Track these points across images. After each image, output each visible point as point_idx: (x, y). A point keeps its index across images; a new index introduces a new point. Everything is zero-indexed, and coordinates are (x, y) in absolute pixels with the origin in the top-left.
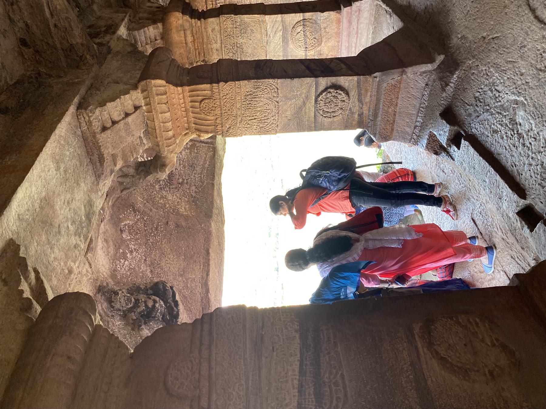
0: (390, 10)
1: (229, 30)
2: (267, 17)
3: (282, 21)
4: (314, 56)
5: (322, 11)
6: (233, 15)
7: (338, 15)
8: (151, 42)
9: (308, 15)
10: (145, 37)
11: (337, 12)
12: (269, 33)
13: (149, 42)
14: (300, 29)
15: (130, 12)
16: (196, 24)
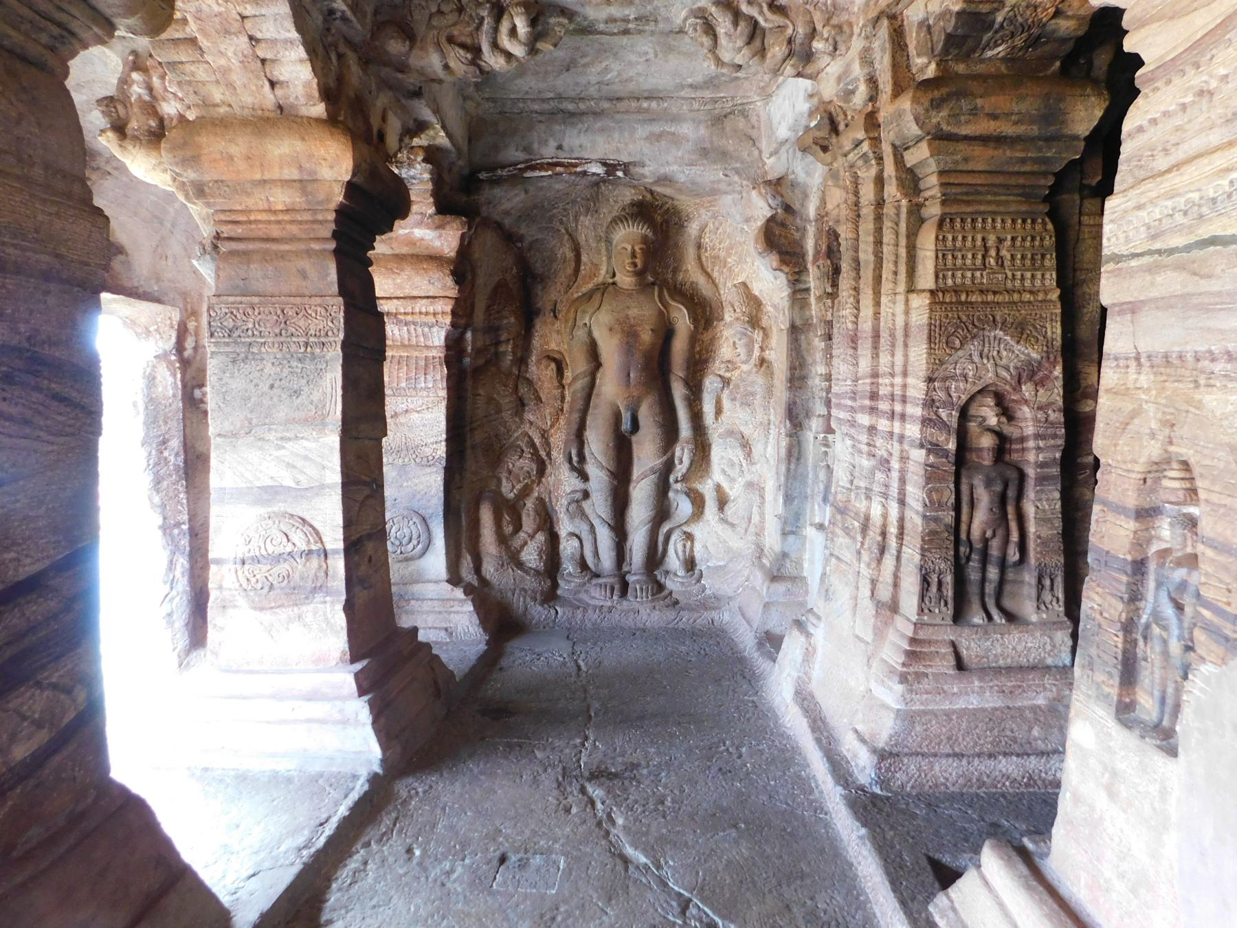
0: (321, 842)
1: (302, 323)
2: (333, 440)
3: (322, 486)
4: (220, 588)
5: (349, 608)
6: (342, 336)
7: (337, 655)
8: (263, 61)
9: (338, 565)
10: (274, 42)
11: (344, 653)
12: (289, 445)
13: (261, 54)
14: (300, 540)
15: (359, 29)
16: (321, 222)
